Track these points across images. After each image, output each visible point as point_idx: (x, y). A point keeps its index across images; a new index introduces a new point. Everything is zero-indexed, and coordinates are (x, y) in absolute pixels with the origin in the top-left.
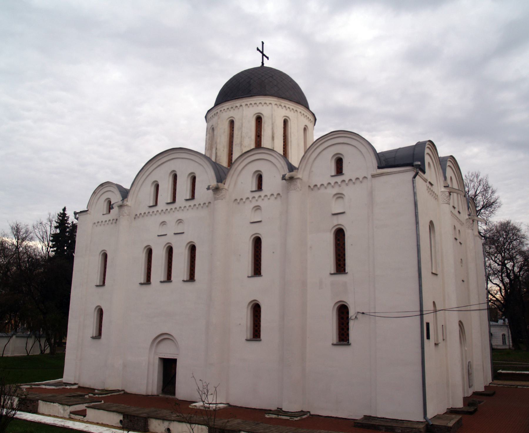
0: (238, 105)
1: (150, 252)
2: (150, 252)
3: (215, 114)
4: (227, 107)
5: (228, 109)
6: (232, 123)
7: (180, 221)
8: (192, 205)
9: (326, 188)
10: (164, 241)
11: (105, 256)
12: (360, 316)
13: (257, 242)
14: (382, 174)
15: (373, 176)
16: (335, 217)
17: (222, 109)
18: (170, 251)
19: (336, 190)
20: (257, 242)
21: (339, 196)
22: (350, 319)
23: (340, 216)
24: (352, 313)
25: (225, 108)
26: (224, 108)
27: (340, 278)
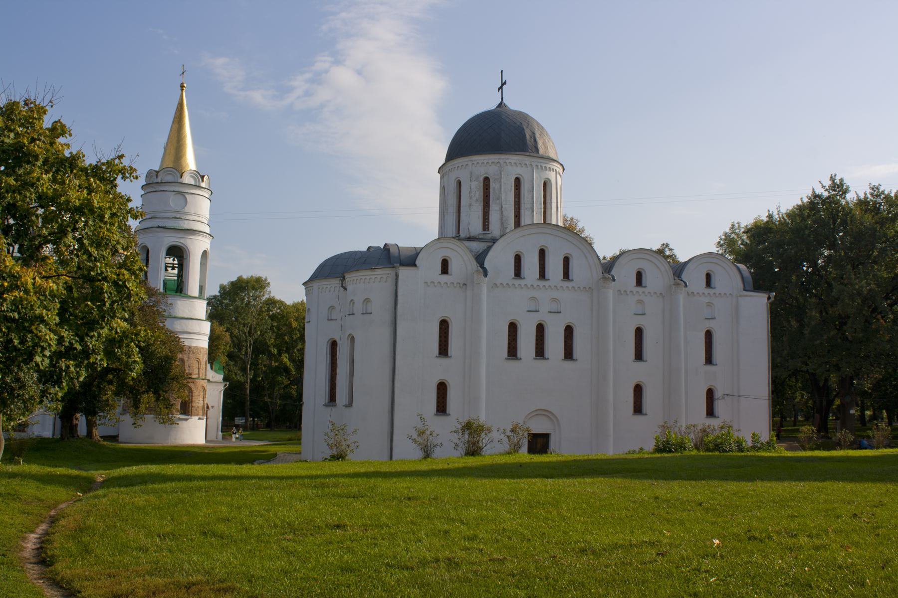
0: (528, 163)
1: (513, 328)
2: (513, 328)
3: (492, 163)
4: (515, 161)
5: (515, 163)
6: (518, 181)
7: (555, 300)
8: (570, 287)
9: (700, 296)
10: (535, 320)
11: (444, 326)
12: (726, 396)
13: (639, 332)
14: (746, 296)
15: (741, 296)
16: (707, 320)
17: (508, 161)
18: (540, 329)
19: (707, 300)
20: (639, 332)
21: (709, 305)
22: (718, 399)
23: (711, 320)
24: (718, 394)
25: (513, 162)
26: (510, 161)
27: (710, 368)
